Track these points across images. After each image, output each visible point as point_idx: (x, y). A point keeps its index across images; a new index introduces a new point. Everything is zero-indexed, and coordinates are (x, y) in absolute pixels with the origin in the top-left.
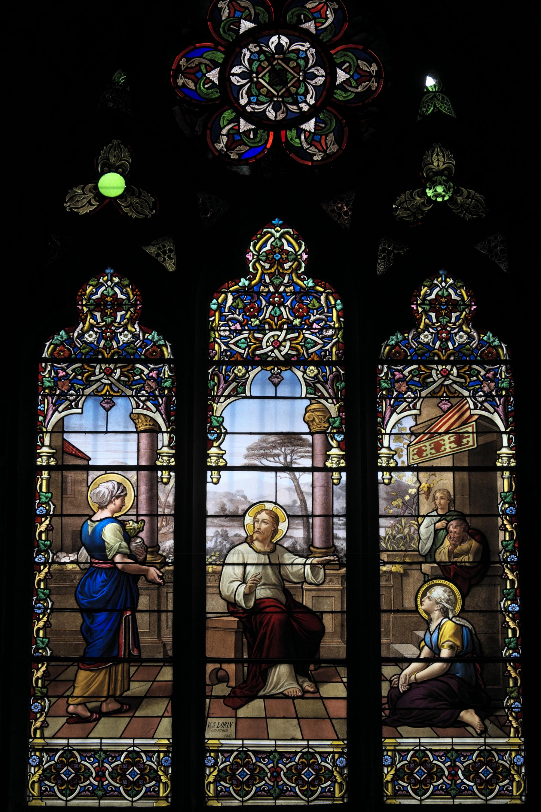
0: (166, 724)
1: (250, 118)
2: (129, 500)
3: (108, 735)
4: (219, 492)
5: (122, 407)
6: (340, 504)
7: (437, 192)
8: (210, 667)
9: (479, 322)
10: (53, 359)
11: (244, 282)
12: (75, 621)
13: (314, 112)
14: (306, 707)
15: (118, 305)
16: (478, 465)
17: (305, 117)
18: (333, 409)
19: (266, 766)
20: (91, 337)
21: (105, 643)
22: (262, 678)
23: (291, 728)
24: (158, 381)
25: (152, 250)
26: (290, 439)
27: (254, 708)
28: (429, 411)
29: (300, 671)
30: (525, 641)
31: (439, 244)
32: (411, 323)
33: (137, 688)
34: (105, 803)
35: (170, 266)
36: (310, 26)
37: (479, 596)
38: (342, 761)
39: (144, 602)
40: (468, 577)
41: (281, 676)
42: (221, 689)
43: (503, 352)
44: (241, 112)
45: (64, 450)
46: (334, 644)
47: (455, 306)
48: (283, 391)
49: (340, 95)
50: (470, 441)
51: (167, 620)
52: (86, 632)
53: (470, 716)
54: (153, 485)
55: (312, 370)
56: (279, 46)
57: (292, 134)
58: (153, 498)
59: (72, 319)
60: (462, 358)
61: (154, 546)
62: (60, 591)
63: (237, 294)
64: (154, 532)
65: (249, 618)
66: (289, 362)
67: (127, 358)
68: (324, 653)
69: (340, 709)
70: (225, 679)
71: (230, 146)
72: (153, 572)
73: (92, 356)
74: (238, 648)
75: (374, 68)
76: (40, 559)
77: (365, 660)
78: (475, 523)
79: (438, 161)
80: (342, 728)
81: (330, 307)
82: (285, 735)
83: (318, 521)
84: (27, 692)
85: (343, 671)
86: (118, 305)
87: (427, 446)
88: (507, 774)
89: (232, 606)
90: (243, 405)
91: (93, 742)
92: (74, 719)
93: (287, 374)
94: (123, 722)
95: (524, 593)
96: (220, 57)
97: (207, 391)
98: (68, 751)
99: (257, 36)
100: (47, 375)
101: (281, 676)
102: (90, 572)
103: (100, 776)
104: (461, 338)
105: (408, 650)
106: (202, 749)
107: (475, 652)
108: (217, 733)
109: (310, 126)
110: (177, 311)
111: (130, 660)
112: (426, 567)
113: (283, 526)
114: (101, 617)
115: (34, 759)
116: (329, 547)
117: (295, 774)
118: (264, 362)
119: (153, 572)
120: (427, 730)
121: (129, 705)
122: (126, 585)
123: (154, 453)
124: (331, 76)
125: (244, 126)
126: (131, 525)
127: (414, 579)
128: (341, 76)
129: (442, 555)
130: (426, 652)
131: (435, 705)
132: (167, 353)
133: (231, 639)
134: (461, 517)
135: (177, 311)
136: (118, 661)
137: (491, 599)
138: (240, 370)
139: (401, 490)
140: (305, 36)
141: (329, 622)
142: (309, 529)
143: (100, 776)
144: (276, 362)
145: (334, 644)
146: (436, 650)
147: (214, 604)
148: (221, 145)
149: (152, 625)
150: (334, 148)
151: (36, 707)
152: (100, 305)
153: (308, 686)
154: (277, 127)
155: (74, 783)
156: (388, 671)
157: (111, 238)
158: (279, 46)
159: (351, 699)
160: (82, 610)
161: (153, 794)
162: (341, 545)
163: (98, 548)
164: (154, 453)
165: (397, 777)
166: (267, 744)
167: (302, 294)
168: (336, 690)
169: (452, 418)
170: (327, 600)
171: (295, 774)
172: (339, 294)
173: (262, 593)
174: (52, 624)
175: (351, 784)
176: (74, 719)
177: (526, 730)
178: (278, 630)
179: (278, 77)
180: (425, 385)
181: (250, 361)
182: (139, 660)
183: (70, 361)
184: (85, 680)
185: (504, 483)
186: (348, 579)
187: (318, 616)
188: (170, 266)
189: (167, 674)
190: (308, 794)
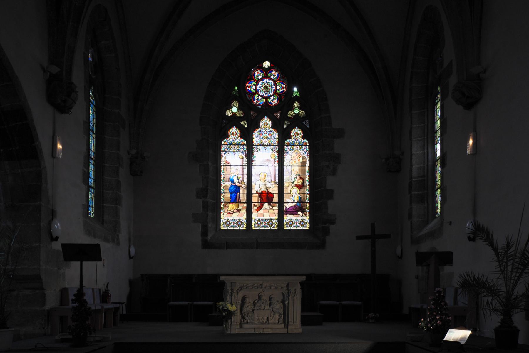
0: (246, 214)
1: (261, 96)
2: (238, 172)
3: (235, 216)
4: (255, 170)
5: (237, 154)
6: (277, 173)
7: (296, 111)
8: (253, 204)
9: (303, 137)
10: (224, 145)
11: (259, 129)
12: (229, 195)
13: (273, 95)
14: (270, 211)
15: (236, 134)
16: (303, 165)
17: (271, 96)
18: (276, 154)
19: (263, 222)
20: (231, 140)
21: (234, 200)
22: (263, 206)
23: (268, 215)
24: (244, 149)
25: (242, 123)
26: (268, 160)
27: (261, 211)
28: (294, 154)
29: (269, 204)
30: (310, 199)
31: (296, 121)
32: (290, 137)
33: (240, 208)
34: (235, 229)
35: (246, 126)
36: (272, 77)
37: (302, 190)
38: (277, 221)
39: (241, 191)
40: (300, 187)
41: (266, 205)
42: (255, 208)
43: (308, 144)
44: (259, 95)
45: (226, 162)
46: (276, 199)
47: (299, 134)
48: (267, 151)
49: (278, 92)
50: (301, 161)
51: (245, 195)
52: (231, 197)
53: (300, 213)
54: (243, 169)
55: (272, 147)
56: (266, 82)
57: (269, 99)
58: (243, 172)
59: (227, 137)
60: (300, 145)
61: (243, 181)
62: (226, 189)
63: (258, 132)
64: (243, 178)
65: (261, 195)
66: (268, 145)
67: (238, 145)
68: (274, 201)
69: (277, 211)
70: (256, 206)
71: (257, 102)
72: (243, 186)
73: (231, 144)
74: (258, 200)
75: (284, 86)
76: (222, 183)
77: (281, 202)
78: (302, 176)
79: (296, 105)
80: (277, 215)
81: (275, 135)
82: (266, 216)
83: (273, 176)
84: (220, 208)
85: (277, 204)
86: (236, 134)
87: (293, 161)
88: (306, 223)
89: (257, 193)
90: (258, 153)
91: (232, 218)
92: (229, 213)
93: (267, 147)
94: (237, 214)
95: (311, 190)
96: (255, 83)
97: (252, 151)
98: (228, 219)
99: (262, 79)
100: (223, 148)
101: (266, 205)
102: (231, 186)
103: (234, 224)
104: (300, 141)
105: (289, 201)
106: (252, 219)
107: (301, 201)
108: (255, 215)
109: (272, 98)
110: (247, 135)
111: (239, 202)
112: (293, 185)
113: (267, 176)
114: (233, 194)
115: (222, 220)
116: (275, 181)
117: (268, 223)
118: (263, 145)
119: (243, 186)
120: (292, 215)
121: (239, 210)
122: (238, 189)
123: (243, 163)
124: (276, 87)
125: (260, 98)
126: (239, 177)
127: (290, 187)
128: (278, 88)
129: (295, 183)
130: (292, 201)
131: (294, 211)
132: (245, 143)
133: (257, 198)
134: (299, 175)
135: (247, 135)
136: (237, 202)
137: (304, 191)
138: (259, 147)
139: (288, 170)
140: (271, 79)
141: (274, 195)
142: (271, 177)
143: (234, 224)
144: (265, 145)
145: (276, 199)
146: (294, 200)
147: (254, 192)
148: (255, 102)
149: (243, 196)
150: (277, 102)
151: (222, 211)
152: (232, 134)
153: (271, 207)
154: (266, 98)
155: (229, 225)
156: (285, 204)
157: (234, 121)
158: (266, 82)
159: (279, 210)
160: (230, 193)
161: (243, 227)
162: (277, 181)
163: (233, 181)
164: (243, 163)
165: (287, 224)
166: (263, 218)
167: (270, 132)
168: (276, 208)
169: (298, 156)
170: (274, 190)
171: (268, 223)
172: (278, 131)
173: (263, 190)
174: (225, 195)
175: (279, 225)
176: (229, 213)
177: (310, 216)
178: (266, 197)
179: (266, 88)
180: (293, 150)
181: (260, 145)
182: (240, 202)
183: (227, 145)
184: (231, 206)
185: (307, 169)
186: (278, 187)
187: (272, 194)
188: (246, 126)
189: (245, 205)
190: (271, 227)
